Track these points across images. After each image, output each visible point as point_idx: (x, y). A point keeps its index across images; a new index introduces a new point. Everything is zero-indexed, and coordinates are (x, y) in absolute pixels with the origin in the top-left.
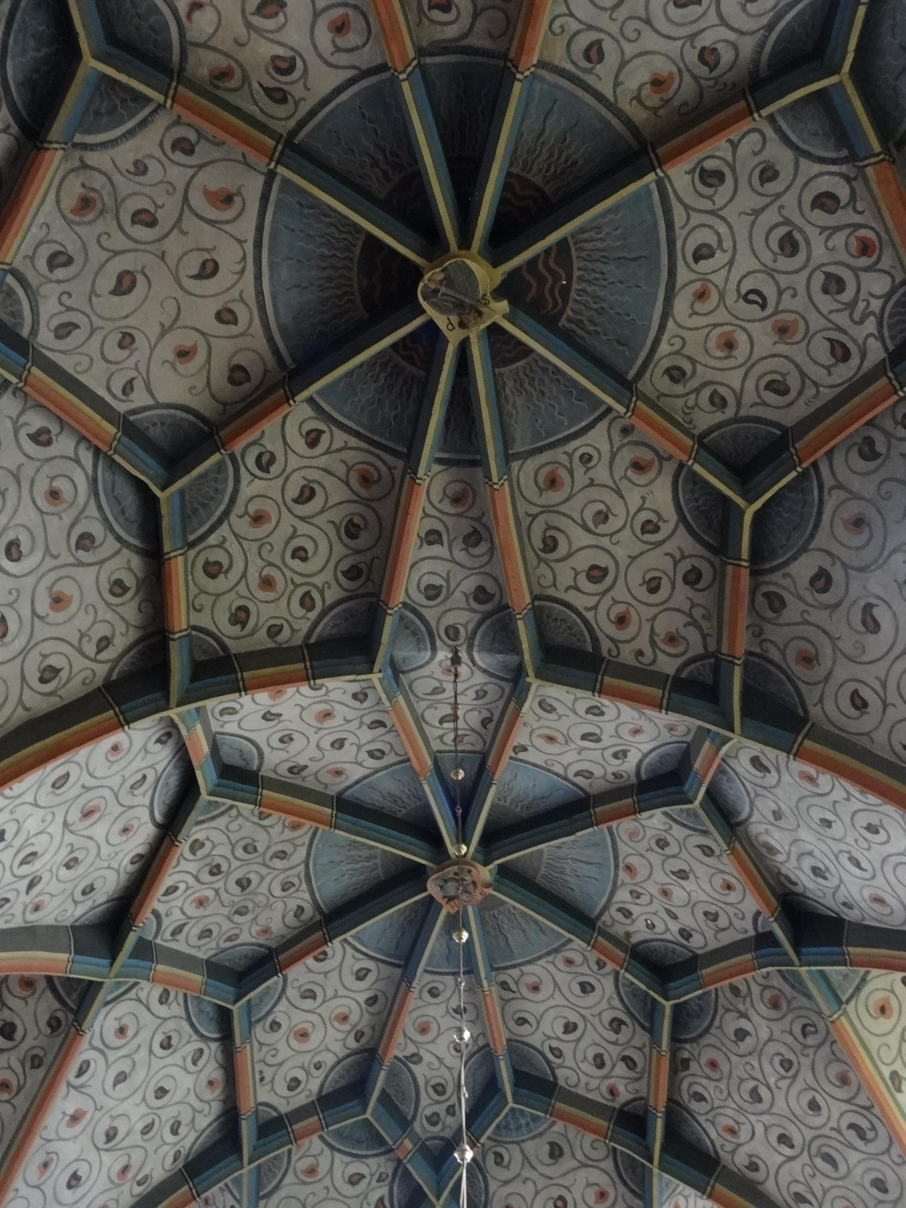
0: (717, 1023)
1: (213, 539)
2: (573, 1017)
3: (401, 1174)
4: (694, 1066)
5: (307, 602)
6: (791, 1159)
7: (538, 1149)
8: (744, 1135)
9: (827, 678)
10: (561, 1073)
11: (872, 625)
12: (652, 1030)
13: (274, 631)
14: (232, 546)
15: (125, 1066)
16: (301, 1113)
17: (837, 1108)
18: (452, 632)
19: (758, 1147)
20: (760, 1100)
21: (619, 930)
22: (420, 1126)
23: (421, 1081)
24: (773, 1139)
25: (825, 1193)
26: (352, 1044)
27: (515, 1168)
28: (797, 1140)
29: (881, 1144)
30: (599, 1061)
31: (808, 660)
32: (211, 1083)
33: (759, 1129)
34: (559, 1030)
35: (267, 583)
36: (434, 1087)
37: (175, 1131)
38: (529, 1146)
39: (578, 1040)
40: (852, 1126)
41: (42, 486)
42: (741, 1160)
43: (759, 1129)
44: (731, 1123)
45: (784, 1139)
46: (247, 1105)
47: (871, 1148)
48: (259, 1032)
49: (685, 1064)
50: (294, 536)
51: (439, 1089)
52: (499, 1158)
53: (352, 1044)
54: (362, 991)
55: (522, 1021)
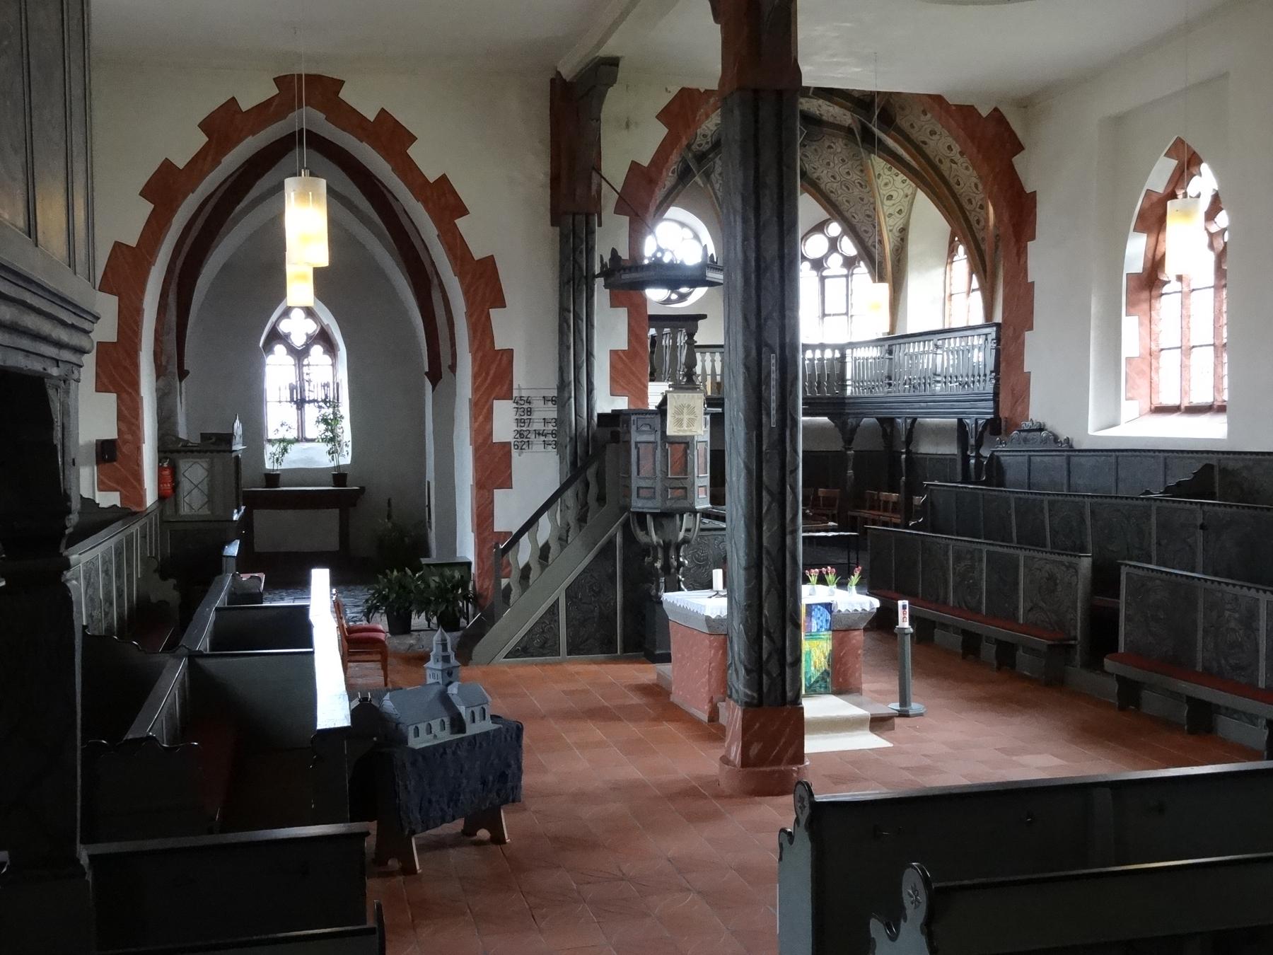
0: (822, 140)
3: (684, 160)
6: (834, 182)
8: (820, 171)
9: (906, 116)
11: (925, 113)
17: (856, 177)
19: (823, 175)
20: (829, 165)
22: (695, 147)
23: (698, 133)
24: (830, 174)
25: (842, 194)
28: (838, 179)
29: (868, 189)
31: (903, 109)
33: (825, 172)
36: (703, 136)
40: (859, 183)
42: (815, 175)
43: (825, 172)
44: (815, 167)
45: (833, 177)
47: (862, 190)
51: (705, 136)
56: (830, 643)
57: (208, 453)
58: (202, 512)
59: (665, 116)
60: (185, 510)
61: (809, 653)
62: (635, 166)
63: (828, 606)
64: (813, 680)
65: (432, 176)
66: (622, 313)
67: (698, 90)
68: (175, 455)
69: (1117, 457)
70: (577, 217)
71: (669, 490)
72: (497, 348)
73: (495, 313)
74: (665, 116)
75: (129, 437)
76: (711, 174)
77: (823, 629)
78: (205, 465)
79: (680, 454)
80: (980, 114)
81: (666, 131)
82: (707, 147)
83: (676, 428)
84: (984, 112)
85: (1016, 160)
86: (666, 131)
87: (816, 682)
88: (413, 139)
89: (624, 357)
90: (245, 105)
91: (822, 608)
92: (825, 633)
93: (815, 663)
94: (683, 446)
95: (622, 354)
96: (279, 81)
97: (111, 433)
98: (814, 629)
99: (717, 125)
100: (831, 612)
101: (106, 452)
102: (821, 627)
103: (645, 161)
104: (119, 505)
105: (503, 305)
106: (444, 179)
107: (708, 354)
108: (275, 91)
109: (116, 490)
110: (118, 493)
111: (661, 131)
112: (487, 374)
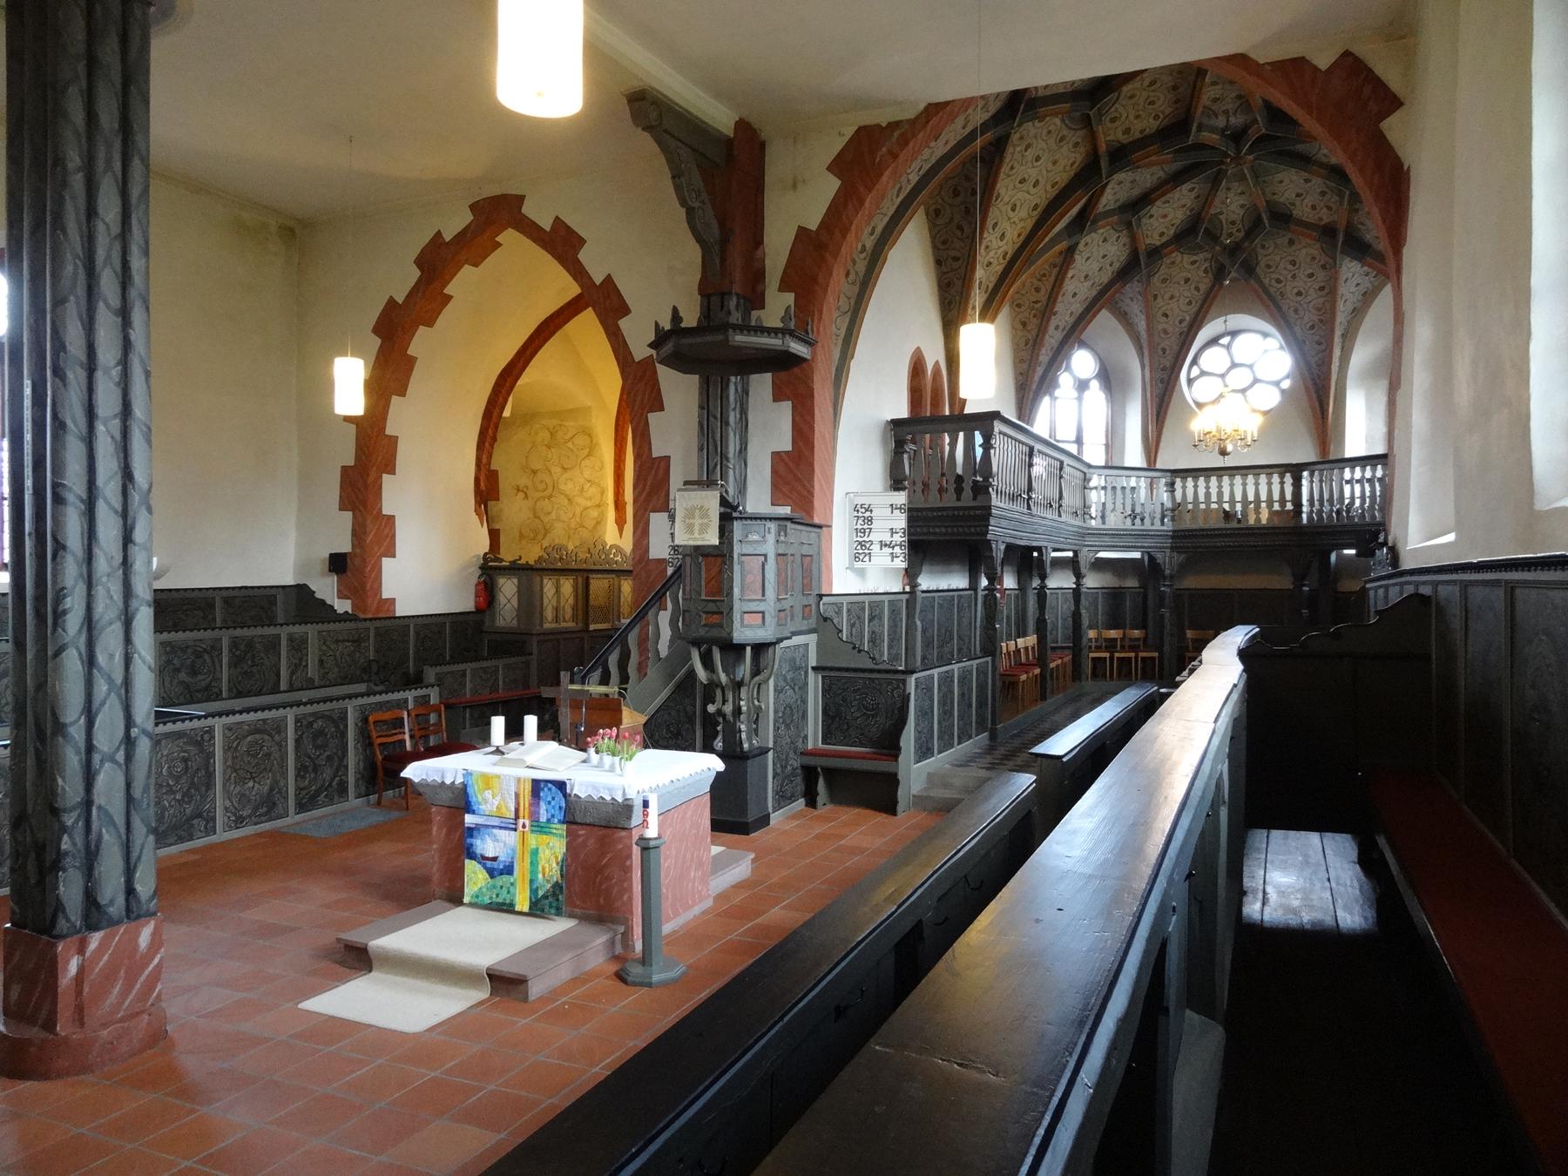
1: (1113, 109)
2: (1300, 191)
4: (1360, 212)
5: (1156, 117)
7: (1285, 241)
10: (1295, 212)
12: (1341, 196)
13: (1141, 132)
14: (1121, 110)
15: (1089, 255)
16: (1165, 245)
18: (1226, 112)
21: (1325, 160)
26: (1188, 213)
27: (1271, 250)
30: (1313, 207)
32: (1125, 245)
34: (1294, 196)
35: (1137, 117)
37: (1111, 265)
38: (1279, 241)
39: (1302, 200)
41: (1045, 131)
46: (1142, 248)
48: (1144, 221)
49: (1357, 211)
50: (1149, 97)
51: (1233, 223)
52: (1263, 247)
53: (1188, 213)
54: (1193, 194)
55: (1274, 194)
56: (564, 841)
57: (517, 572)
58: (512, 625)
59: (839, 166)
60: (501, 622)
61: (535, 852)
62: (802, 232)
63: (561, 785)
64: (541, 893)
65: (598, 279)
66: (786, 408)
67: (879, 126)
68: (491, 572)
69: (1511, 588)
70: (712, 299)
71: (704, 616)
72: (655, 455)
73: (653, 418)
74: (837, 166)
75: (358, 551)
76: (1255, 269)
77: (556, 821)
78: (515, 581)
79: (714, 572)
80: (1316, 69)
81: (839, 182)
82: (1242, 234)
83: (687, 536)
84: (1323, 61)
85: (1392, 127)
86: (839, 182)
87: (545, 897)
88: (582, 242)
89: (787, 460)
90: (448, 236)
91: (554, 788)
92: (558, 826)
93: (544, 869)
94: (719, 559)
95: (785, 457)
96: (473, 207)
97: (345, 547)
98: (543, 819)
99: (1242, 206)
100: (565, 795)
101: (338, 563)
102: (553, 816)
103: (813, 225)
104: (350, 612)
105: (661, 409)
106: (609, 280)
107: (1250, 477)
108: (469, 217)
109: (349, 598)
110: (350, 601)
111: (834, 184)
112: (644, 488)
